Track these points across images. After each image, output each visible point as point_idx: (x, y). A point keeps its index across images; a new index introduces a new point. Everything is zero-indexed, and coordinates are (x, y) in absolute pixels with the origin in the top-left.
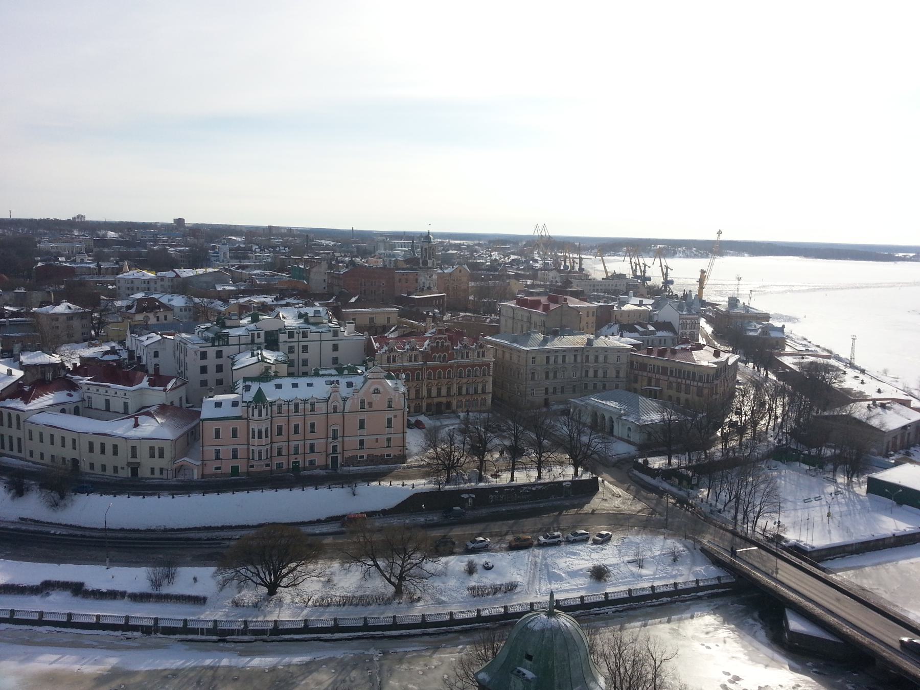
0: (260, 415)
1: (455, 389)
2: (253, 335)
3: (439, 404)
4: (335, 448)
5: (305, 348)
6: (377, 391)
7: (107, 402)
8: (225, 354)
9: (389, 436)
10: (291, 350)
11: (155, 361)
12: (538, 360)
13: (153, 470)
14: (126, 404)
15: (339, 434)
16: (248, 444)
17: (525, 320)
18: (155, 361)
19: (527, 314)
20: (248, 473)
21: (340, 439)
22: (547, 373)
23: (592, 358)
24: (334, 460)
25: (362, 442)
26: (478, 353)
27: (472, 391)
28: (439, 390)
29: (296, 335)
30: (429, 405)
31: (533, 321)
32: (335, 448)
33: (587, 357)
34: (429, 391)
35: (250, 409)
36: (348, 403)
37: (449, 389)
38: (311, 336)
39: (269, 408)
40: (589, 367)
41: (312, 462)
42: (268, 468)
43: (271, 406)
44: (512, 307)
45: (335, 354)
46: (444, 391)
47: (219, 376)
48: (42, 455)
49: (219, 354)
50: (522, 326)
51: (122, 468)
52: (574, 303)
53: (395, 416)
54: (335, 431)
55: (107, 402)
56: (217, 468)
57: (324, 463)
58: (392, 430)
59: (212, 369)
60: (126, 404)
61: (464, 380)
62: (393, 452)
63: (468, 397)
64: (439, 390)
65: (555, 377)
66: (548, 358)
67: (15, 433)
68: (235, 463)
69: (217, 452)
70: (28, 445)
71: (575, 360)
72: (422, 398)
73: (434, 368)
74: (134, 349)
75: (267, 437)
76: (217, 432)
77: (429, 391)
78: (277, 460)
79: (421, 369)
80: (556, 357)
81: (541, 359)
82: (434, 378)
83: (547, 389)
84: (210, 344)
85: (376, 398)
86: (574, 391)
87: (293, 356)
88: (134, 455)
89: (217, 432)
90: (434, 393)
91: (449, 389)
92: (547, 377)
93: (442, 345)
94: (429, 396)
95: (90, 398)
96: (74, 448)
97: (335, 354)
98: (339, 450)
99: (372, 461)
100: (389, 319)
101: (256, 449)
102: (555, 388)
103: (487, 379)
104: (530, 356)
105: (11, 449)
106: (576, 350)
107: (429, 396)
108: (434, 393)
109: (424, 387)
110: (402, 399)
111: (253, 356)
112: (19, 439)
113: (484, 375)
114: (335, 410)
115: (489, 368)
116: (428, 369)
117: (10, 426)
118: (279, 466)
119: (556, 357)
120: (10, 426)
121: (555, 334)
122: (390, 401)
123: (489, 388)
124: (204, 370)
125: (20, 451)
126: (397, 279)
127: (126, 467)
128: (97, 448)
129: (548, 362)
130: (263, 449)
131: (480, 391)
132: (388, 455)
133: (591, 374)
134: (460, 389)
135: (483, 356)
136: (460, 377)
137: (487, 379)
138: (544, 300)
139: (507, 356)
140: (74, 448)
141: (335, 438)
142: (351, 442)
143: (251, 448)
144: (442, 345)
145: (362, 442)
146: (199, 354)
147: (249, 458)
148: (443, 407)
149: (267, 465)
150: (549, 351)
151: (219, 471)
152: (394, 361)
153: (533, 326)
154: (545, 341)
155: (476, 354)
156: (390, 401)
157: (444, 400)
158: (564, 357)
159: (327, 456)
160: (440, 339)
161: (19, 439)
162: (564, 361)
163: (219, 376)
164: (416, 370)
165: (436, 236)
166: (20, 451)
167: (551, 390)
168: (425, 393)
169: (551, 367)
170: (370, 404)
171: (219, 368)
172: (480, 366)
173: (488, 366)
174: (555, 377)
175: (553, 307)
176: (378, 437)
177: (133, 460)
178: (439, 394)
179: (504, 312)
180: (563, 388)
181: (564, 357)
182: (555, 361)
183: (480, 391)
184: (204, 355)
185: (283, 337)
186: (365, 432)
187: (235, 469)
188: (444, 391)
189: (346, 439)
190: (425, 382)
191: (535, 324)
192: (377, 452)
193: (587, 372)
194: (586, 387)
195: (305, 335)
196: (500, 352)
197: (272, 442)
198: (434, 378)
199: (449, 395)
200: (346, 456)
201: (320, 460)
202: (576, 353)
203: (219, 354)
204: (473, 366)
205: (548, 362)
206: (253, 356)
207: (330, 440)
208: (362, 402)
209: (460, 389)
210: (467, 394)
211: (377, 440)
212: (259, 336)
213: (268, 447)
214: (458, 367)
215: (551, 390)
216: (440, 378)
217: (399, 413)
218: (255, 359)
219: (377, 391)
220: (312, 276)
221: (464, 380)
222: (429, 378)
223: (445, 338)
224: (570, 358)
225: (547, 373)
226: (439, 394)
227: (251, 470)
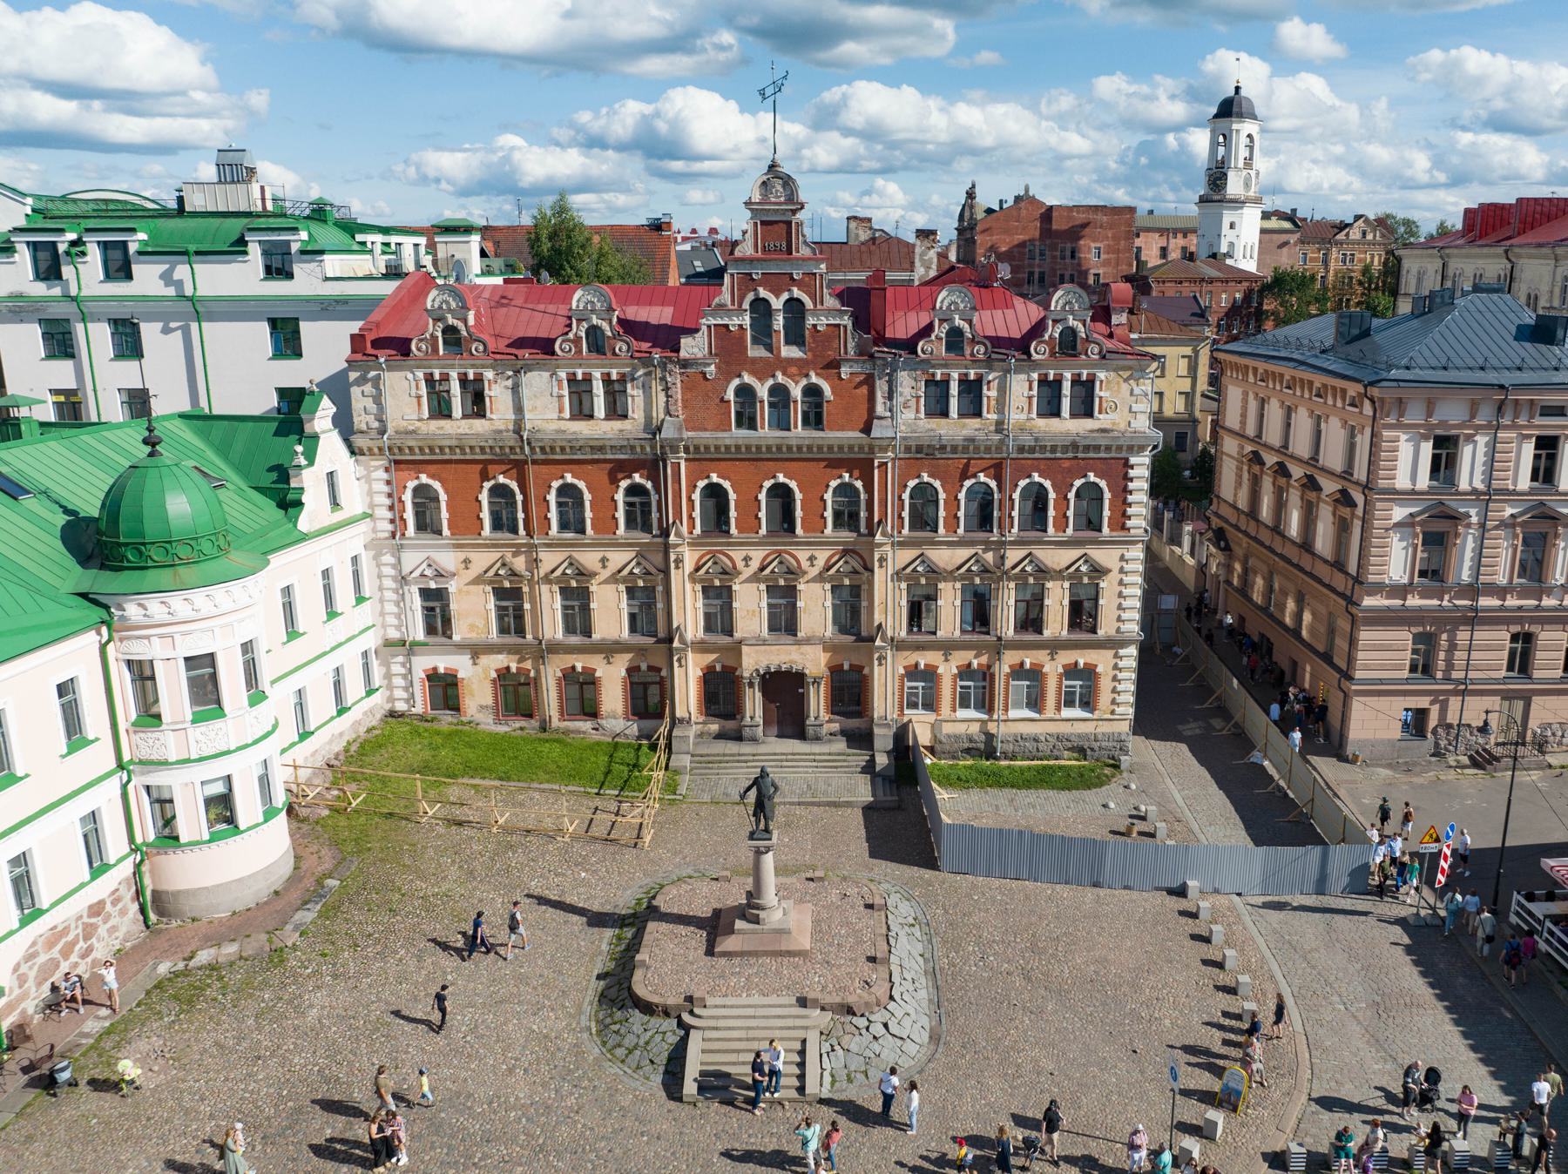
103: (1102, 556)
113: (1091, 523)
115: (1121, 492)
137: (1102, 556)
178: (784, 622)
226: (784, 622)
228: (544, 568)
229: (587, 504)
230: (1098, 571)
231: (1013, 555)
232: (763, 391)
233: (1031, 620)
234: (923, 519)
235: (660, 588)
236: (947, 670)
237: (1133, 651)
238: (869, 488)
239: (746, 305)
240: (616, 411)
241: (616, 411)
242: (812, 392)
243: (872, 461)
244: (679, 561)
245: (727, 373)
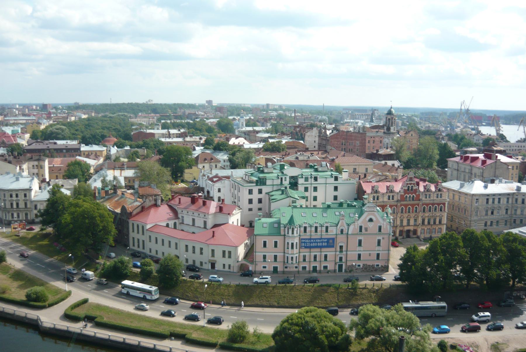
0: (293, 233)
1: (420, 221)
2: (282, 178)
3: (408, 231)
4: (341, 259)
5: (315, 189)
6: (371, 220)
7: (194, 220)
8: (264, 191)
9: (378, 252)
10: (306, 189)
11: (219, 194)
12: (480, 201)
13: (224, 265)
14: (205, 223)
15: (344, 249)
16: (284, 252)
17: (467, 171)
18: (219, 194)
19: (469, 168)
20: (284, 272)
21: (344, 253)
22: (487, 211)
23: (520, 201)
24: (340, 266)
25: (359, 256)
26: (438, 195)
27: (432, 222)
28: (409, 221)
29: (310, 179)
30: (401, 232)
31: (473, 172)
32: (341, 259)
33: (517, 200)
34: (402, 221)
35: (286, 229)
36: (351, 228)
38: (319, 181)
39: (299, 229)
40: (517, 207)
41: (315, 268)
42: (297, 270)
43: (300, 227)
44: (457, 162)
45: (336, 193)
46: (412, 222)
47: (260, 206)
48: (157, 251)
49: (260, 192)
50: (465, 175)
51: (206, 263)
52: (502, 158)
53: (383, 238)
54: (341, 247)
55: (194, 220)
56: (265, 267)
57: (333, 269)
58: (380, 248)
59: (255, 201)
60: (205, 223)
62: (381, 263)
63: (429, 227)
65: (492, 213)
66: (488, 199)
67: (141, 237)
68: (275, 265)
69: (265, 257)
70: (148, 245)
71: (508, 202)
72: (396, 227)
73: (406, 206)
74: (204, 186)
75: (296, 248)
76: (265, 243)
77: (402, 221)
78: (302, 265)
79: (396, 206)
80: (494, 199)
81: (483, 201)
82: (406, 212)
84: (255, 184)
85: (370, 225)
86: (506, 224)
87: (307, 194)
88: (213, 255)
89: (265, 243)
90: (405, 223)
91: (415, 220)
92: (487, 215)
93: (412, 189)
94: (402, 225)
95: (183, 217)
96: (176, 248)
97: (336, 193)
98: (344, 260)
99: (366, 268)
100: (367, 169)
101: (290, 256)
102: (492, 222)
103: (443, 214)
104: (475, 198)
105: (139, 247)
106: (509, 194)
107: (402, 225)
108: (405, 223)
110: (389, 227)
111: (282, 194)
112: (143, 241)
113: (441, 210)
114: (342, 231)
115: (445, 206)
116: (401, 205)
117: (138, 233)
118: (304, 268)
119: (494, 199)
120: (138, 233)
121: (493, 182)
122: (380, 229)
123: (444, 221)
124: (251, 201)
125: (144, 248)
126: (367, 141)
127: (208, 263)
128: (190, 249)
129: (487, 202)
130: (294, 256)
131: (437, 222)
132: (378, 265)
133: (519, 212)
134: (423, 221)
135: (441, 197)
136: (424, 211)
138: (481, 156)
139: (457, 198)
140: (176, 248)
141: (341, 251)
142: (352, 255)
143: (286, 255)
144: (412, 189)
145: (359, 256)
146: (248, 191)
147: (284, 262)
148: (411, 234)
149: (296, 267)
150: (488, 195)
151: (264, 269)
152: (378, 199)
153: (473, 176)
154: (486, 187)
155: (435, 195)
156: (380, 229)
157: (412, 228)
158: (499, 199)
159: (336, 264)
160: (411, 184)
161: (143, 241)
162: (499, 202)
163: (260, 206)
165: (397, 109)
166: (144, 248)
167: (489, 223)
168: (399, 223)
169: (489, 207)
170: (366, 229)
171: (260, 201)
172: (438, 204)
173: (444, 204)
174: (492, 213)
175: (489, 162)
176: (371, 252)
177: (212, 259)
178: (408, 224)
179: (450, 164)
180: (497, 222)
181: (499, 199)
182: (493, 202)
183: (437, 222)
184: (251, 192)
185: (301, 181)
186: (361, 248)
187: (275, 269)
188: (412, 222)
189: (348, 253)
190: (399, 215)
191: (475, 174)
192: (370, 263)
193: (516, 210)
194: (515, 222)
195: (316, 179)
196: (451, 195)
197: (300, 252)
198: (406, 212)
199: (415, 225)
200: (349, 264)
201: (331, 266)
202: (508, 196)
203: (260, 192)
204: (433, 204)
205: (487, 202)
206: (282, 194)
207: (338, 253)
208: (361, 228)
209: (423, 221)
210: (429, 223)
211: (370, 255)
212: (285, 180)
213: (297, 255)
214: (423, 204)
215: (489, 223)
216: (409, 212)
217: (386, 236)
218: (283, 196)
219: (371, 220)
220: (306, 138)
221: (427, 214)
222: (402, 212)
223: (414, 184)
224: (504, 201)
225: (487, 211)
226: (408, 224)
227: (286, 270)
230: (442, 216)
232: (408, 196)
233: (435, 223)
234: (424, 211)
236: (426, 229)
237: (445, 226)
240: (393, 199)
241: (393, 199)
242: (413, 196)
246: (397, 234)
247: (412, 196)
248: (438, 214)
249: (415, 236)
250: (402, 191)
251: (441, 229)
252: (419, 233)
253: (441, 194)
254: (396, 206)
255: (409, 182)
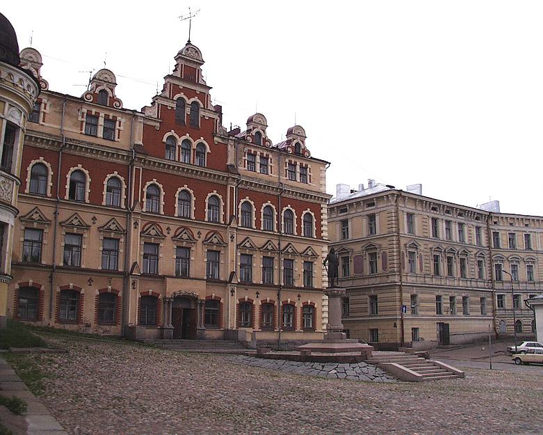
28: (184, 253)
30: (149, 302)
37: (214, 256)
46: (198, 262)
61: (259, 241)
63: (269, 296)
64: (184, 253)
83: (439, 298)
90: (167, 261)
91: (214, 256)
108: (167, 261)
109: (135, 235)
157: (200, 290)
164: (112, 167)
178: (184, 274)
188: (198, 262)
209: (247, 266)
225: (436, 259)
228: (61, 218)
229: (88, 184)
231: (283, 245)
232: (180, 141)
235: (122, 240)
238: (225, 201)
239: (175, 98)
243: (226, 186)
244: (136, 224)
245: (164, 128)
246: (133, 317)
247: (194, 144)
248: (300, 248)
249: (213, 334)
250: (153, 113)
251: (312, 307)
252: (231, 318)
253: (304, 168)
254: (126, 171)
255: (182, 85)
